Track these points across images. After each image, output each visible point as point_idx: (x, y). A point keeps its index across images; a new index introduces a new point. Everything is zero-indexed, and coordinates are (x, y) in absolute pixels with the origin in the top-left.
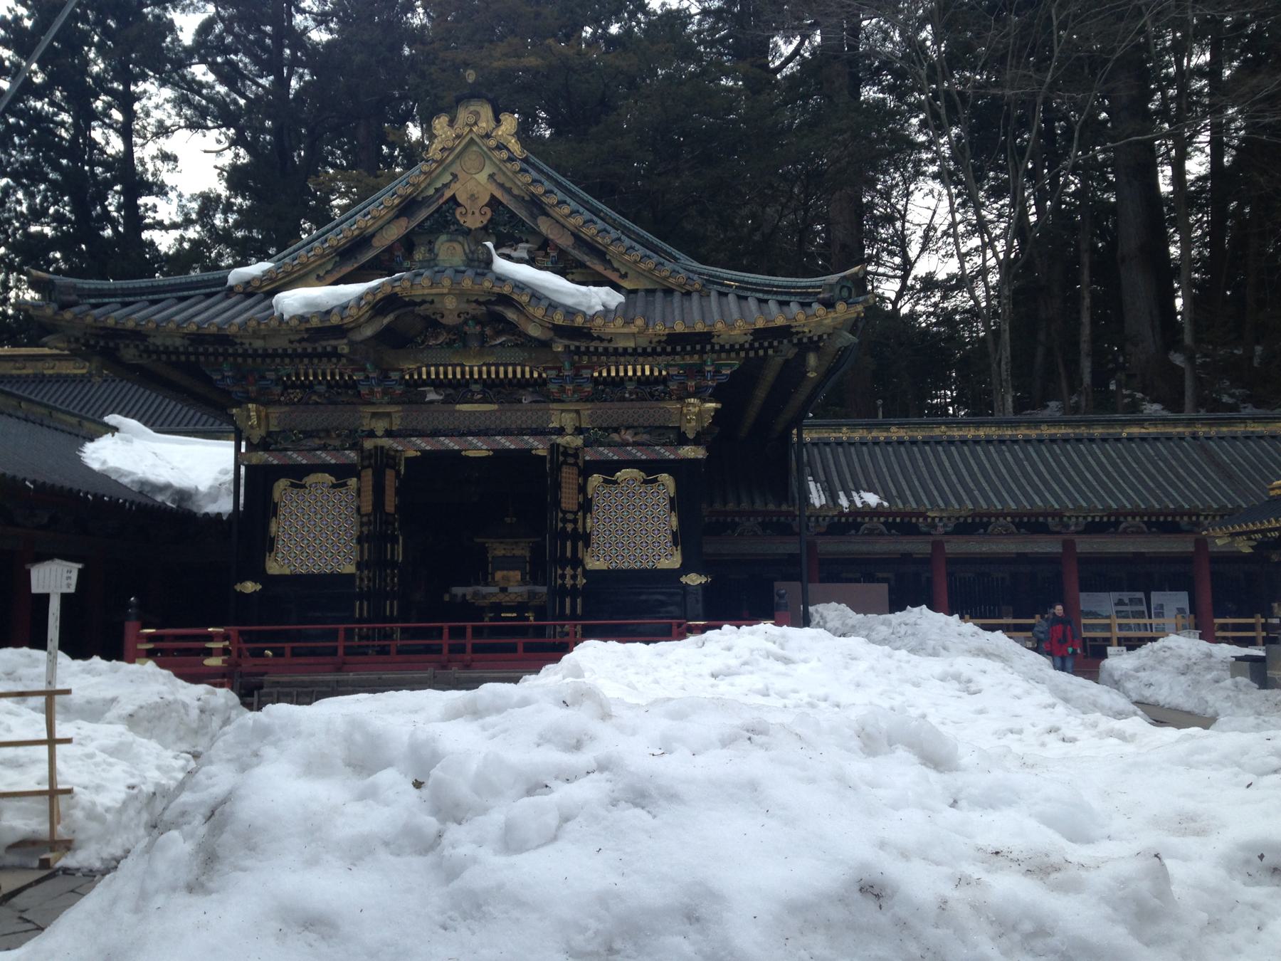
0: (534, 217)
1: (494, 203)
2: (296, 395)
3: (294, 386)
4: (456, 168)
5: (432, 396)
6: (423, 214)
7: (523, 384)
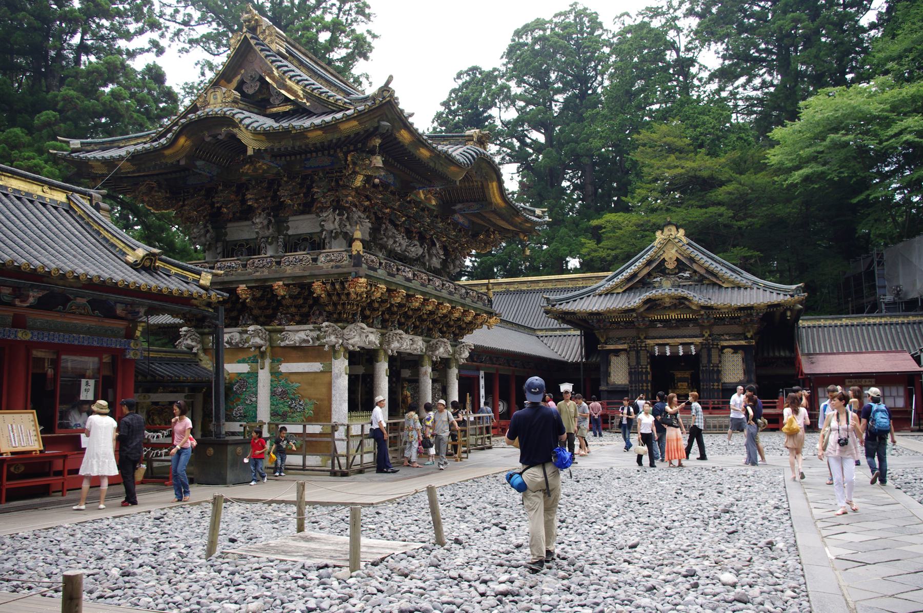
0: (692, 264)
1: (677, 260)
2: (615, 326)
3: (614, 323)
4: (664, 249)
5: (659, 325)
6: (654, 265)
7: (689, 320)
